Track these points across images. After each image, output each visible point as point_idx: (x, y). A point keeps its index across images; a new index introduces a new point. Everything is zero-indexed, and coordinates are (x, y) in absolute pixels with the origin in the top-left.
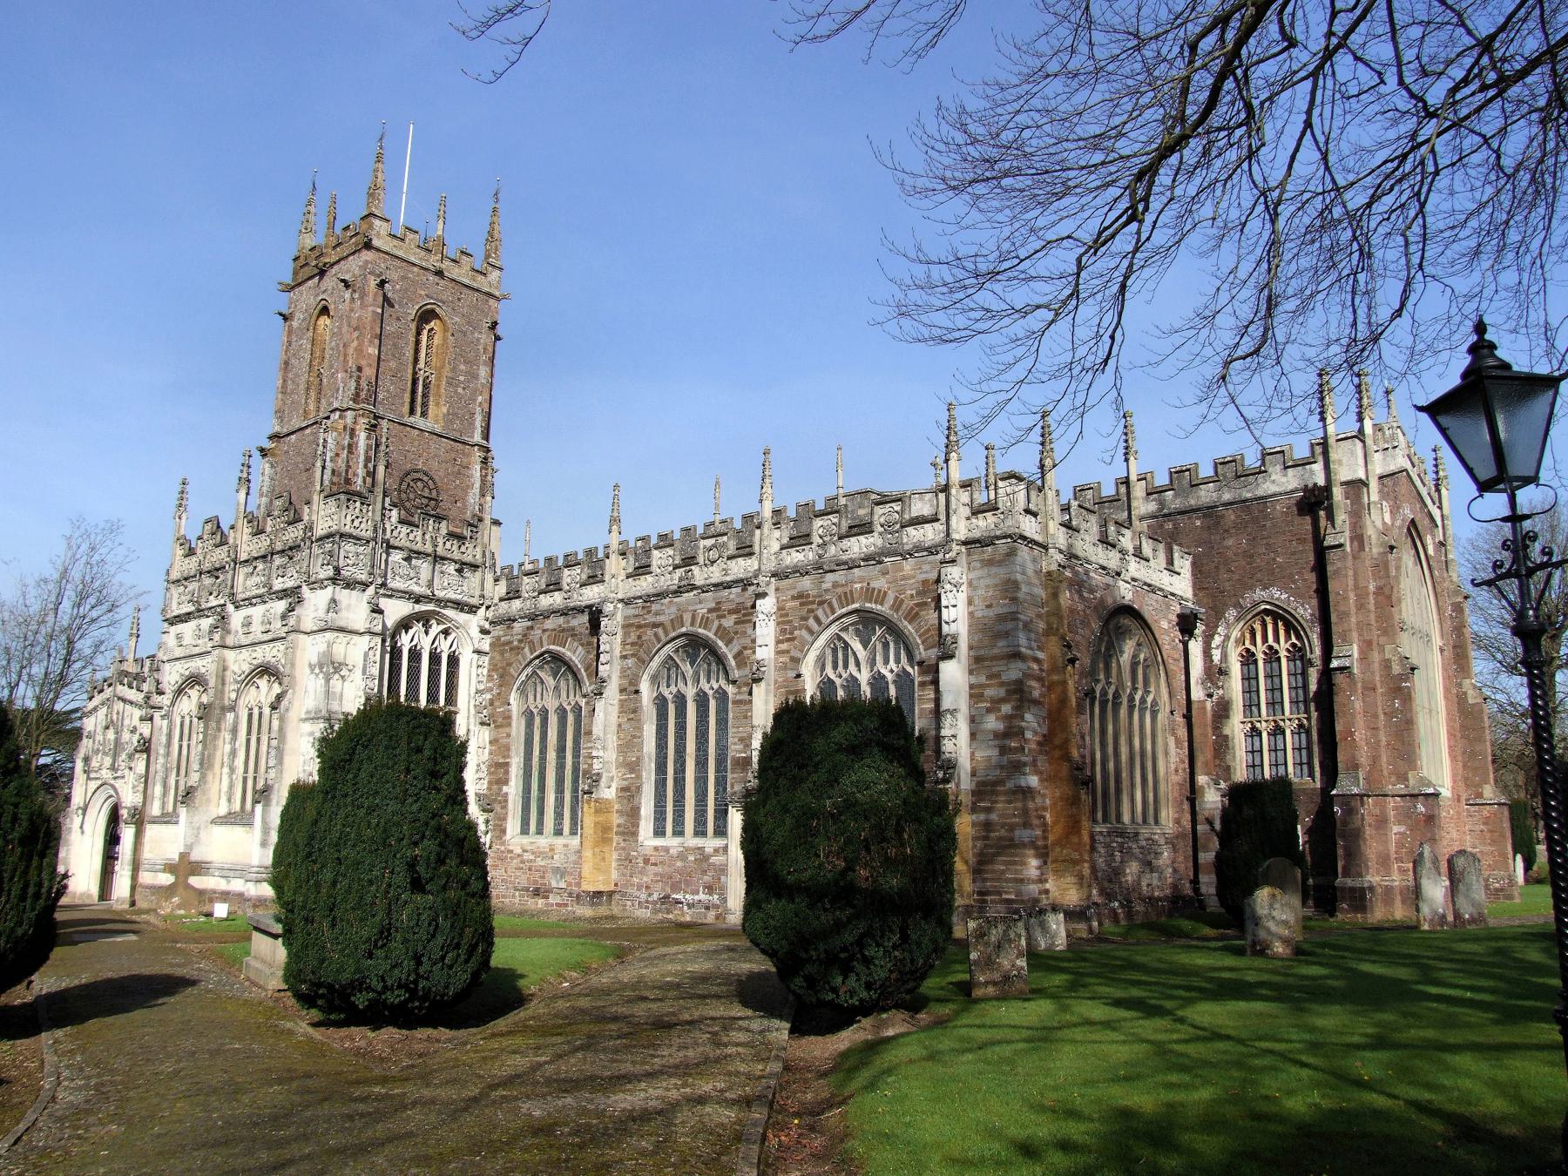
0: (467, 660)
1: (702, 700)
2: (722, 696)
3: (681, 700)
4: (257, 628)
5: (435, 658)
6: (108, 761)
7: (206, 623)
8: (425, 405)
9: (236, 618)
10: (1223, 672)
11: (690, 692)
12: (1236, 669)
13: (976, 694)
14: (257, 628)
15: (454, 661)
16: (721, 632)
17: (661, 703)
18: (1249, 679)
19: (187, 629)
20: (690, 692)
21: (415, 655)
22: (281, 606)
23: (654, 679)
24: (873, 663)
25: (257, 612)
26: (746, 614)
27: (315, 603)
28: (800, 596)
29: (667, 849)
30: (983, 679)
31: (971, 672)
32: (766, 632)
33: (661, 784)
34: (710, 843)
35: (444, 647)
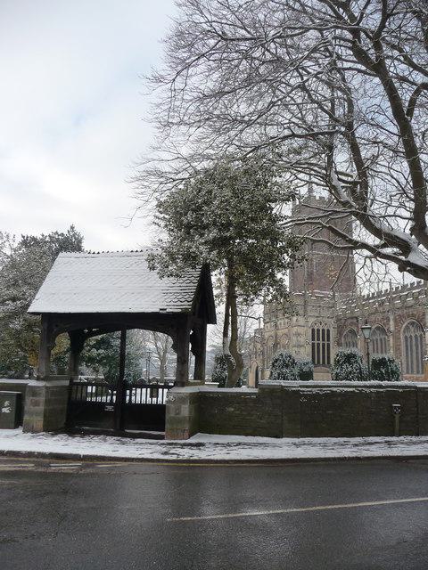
0: (331, 329)
1: (381, 340)
5: (323, 330)
9: (278, 323)
15: (328, 331)
19: (268, 325)
21: (318, 330)
22: (287, 320)
32: (392, 323)
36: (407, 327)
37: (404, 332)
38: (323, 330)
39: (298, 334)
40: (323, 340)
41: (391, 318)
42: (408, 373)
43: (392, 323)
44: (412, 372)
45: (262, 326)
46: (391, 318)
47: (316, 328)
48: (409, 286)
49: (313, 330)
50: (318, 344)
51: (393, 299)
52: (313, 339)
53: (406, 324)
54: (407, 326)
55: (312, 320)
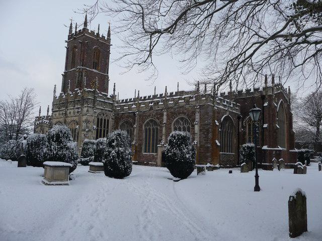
0: (110, 120)
1: (153, 129)
2: (157, 129)
3: (150, 129)
4: (72, 114)
5: (105, 120)
7: (61, 112)
8: (96, 65)
9: (68, 112)
10: (246, 127)
11: (151, 128)
12: (247, 127)
13: (200, 130)
14: (72, 114)
15: (108, 121)
16: (158, 118)
17: (146, 129)
18: (249, 128)
20: (151, 128)
21: (101, 119)
22: (77, 110)
24: (183, 124)
25: (72, 111)
26: (162, 115)
27: (85, 109)
29: (147, 155)
31: (200, 127)
32: (165, 117)
33: (146, 143)
34: (155, 154)
36: (177, 121)
37: (174, 124)
38: (105, 120)
39: (87, 121)
40: (104, 127)
41: (165, 113)
42: (145, 152)
43: (165, 117)
44: (149, 152)
45: (50, 113)
46: (165, 113)
47: (100, 118)
48: (143, 98)
49: (98, 119)
50: (101, 130)
51: (158, 102)
52: (98, 126)
53: (177, 118)
54: (122, 124)
55: (98, 111)
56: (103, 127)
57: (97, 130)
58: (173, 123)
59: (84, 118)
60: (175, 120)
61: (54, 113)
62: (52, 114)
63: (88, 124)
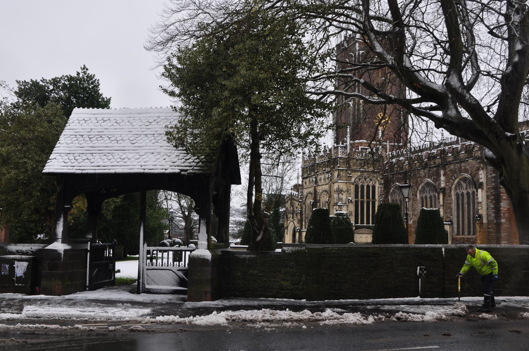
0: (377, 185)
1: (431, 197)
3: (426, 197)
5: (368, 187)
6: (291, 216)
11: (428, 196)
15: (374, 187)
17: (422, 198)
19: (307, 180)
20: (428, 196)
21: (362, 187)
22: (327, 175)
23: (420, 192)
24: (467, 189)
28: (450, 170)
30: (489, 194)
35: (371, 184)
36: (459, 184)
37: (456, 189)
41: (442, 172)
43: (442, 178)
45: (300, 183)
46: (442, 172)
49: (357, 187)
52: (356, 196)
54: (458, 182)
56: (365, 197)
57: (357, 202)
58: (453, 187)
59: (336, 186)
60: (456, 182)
61: (304, 180)
62: (302, 181)
63: (340, 195)
